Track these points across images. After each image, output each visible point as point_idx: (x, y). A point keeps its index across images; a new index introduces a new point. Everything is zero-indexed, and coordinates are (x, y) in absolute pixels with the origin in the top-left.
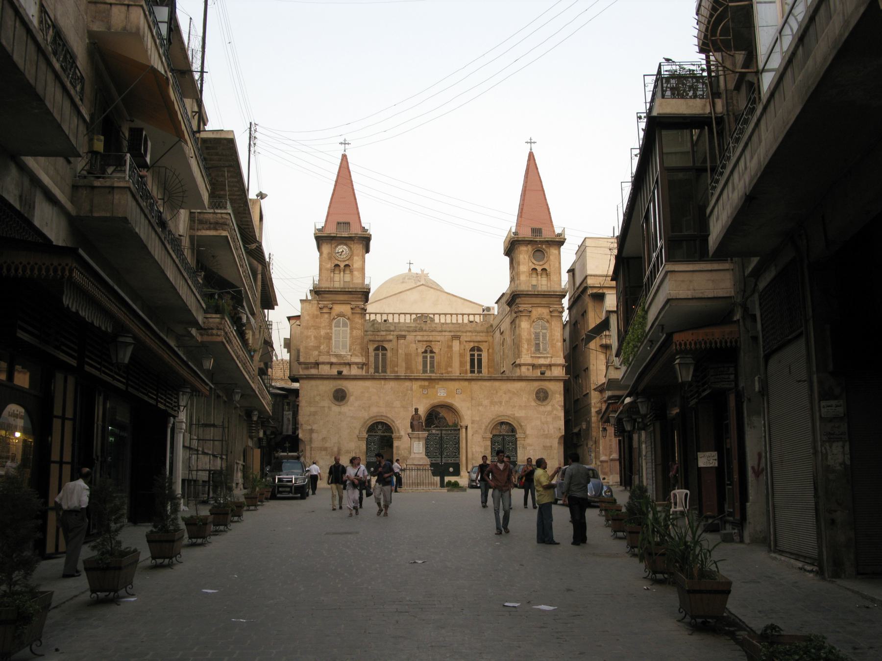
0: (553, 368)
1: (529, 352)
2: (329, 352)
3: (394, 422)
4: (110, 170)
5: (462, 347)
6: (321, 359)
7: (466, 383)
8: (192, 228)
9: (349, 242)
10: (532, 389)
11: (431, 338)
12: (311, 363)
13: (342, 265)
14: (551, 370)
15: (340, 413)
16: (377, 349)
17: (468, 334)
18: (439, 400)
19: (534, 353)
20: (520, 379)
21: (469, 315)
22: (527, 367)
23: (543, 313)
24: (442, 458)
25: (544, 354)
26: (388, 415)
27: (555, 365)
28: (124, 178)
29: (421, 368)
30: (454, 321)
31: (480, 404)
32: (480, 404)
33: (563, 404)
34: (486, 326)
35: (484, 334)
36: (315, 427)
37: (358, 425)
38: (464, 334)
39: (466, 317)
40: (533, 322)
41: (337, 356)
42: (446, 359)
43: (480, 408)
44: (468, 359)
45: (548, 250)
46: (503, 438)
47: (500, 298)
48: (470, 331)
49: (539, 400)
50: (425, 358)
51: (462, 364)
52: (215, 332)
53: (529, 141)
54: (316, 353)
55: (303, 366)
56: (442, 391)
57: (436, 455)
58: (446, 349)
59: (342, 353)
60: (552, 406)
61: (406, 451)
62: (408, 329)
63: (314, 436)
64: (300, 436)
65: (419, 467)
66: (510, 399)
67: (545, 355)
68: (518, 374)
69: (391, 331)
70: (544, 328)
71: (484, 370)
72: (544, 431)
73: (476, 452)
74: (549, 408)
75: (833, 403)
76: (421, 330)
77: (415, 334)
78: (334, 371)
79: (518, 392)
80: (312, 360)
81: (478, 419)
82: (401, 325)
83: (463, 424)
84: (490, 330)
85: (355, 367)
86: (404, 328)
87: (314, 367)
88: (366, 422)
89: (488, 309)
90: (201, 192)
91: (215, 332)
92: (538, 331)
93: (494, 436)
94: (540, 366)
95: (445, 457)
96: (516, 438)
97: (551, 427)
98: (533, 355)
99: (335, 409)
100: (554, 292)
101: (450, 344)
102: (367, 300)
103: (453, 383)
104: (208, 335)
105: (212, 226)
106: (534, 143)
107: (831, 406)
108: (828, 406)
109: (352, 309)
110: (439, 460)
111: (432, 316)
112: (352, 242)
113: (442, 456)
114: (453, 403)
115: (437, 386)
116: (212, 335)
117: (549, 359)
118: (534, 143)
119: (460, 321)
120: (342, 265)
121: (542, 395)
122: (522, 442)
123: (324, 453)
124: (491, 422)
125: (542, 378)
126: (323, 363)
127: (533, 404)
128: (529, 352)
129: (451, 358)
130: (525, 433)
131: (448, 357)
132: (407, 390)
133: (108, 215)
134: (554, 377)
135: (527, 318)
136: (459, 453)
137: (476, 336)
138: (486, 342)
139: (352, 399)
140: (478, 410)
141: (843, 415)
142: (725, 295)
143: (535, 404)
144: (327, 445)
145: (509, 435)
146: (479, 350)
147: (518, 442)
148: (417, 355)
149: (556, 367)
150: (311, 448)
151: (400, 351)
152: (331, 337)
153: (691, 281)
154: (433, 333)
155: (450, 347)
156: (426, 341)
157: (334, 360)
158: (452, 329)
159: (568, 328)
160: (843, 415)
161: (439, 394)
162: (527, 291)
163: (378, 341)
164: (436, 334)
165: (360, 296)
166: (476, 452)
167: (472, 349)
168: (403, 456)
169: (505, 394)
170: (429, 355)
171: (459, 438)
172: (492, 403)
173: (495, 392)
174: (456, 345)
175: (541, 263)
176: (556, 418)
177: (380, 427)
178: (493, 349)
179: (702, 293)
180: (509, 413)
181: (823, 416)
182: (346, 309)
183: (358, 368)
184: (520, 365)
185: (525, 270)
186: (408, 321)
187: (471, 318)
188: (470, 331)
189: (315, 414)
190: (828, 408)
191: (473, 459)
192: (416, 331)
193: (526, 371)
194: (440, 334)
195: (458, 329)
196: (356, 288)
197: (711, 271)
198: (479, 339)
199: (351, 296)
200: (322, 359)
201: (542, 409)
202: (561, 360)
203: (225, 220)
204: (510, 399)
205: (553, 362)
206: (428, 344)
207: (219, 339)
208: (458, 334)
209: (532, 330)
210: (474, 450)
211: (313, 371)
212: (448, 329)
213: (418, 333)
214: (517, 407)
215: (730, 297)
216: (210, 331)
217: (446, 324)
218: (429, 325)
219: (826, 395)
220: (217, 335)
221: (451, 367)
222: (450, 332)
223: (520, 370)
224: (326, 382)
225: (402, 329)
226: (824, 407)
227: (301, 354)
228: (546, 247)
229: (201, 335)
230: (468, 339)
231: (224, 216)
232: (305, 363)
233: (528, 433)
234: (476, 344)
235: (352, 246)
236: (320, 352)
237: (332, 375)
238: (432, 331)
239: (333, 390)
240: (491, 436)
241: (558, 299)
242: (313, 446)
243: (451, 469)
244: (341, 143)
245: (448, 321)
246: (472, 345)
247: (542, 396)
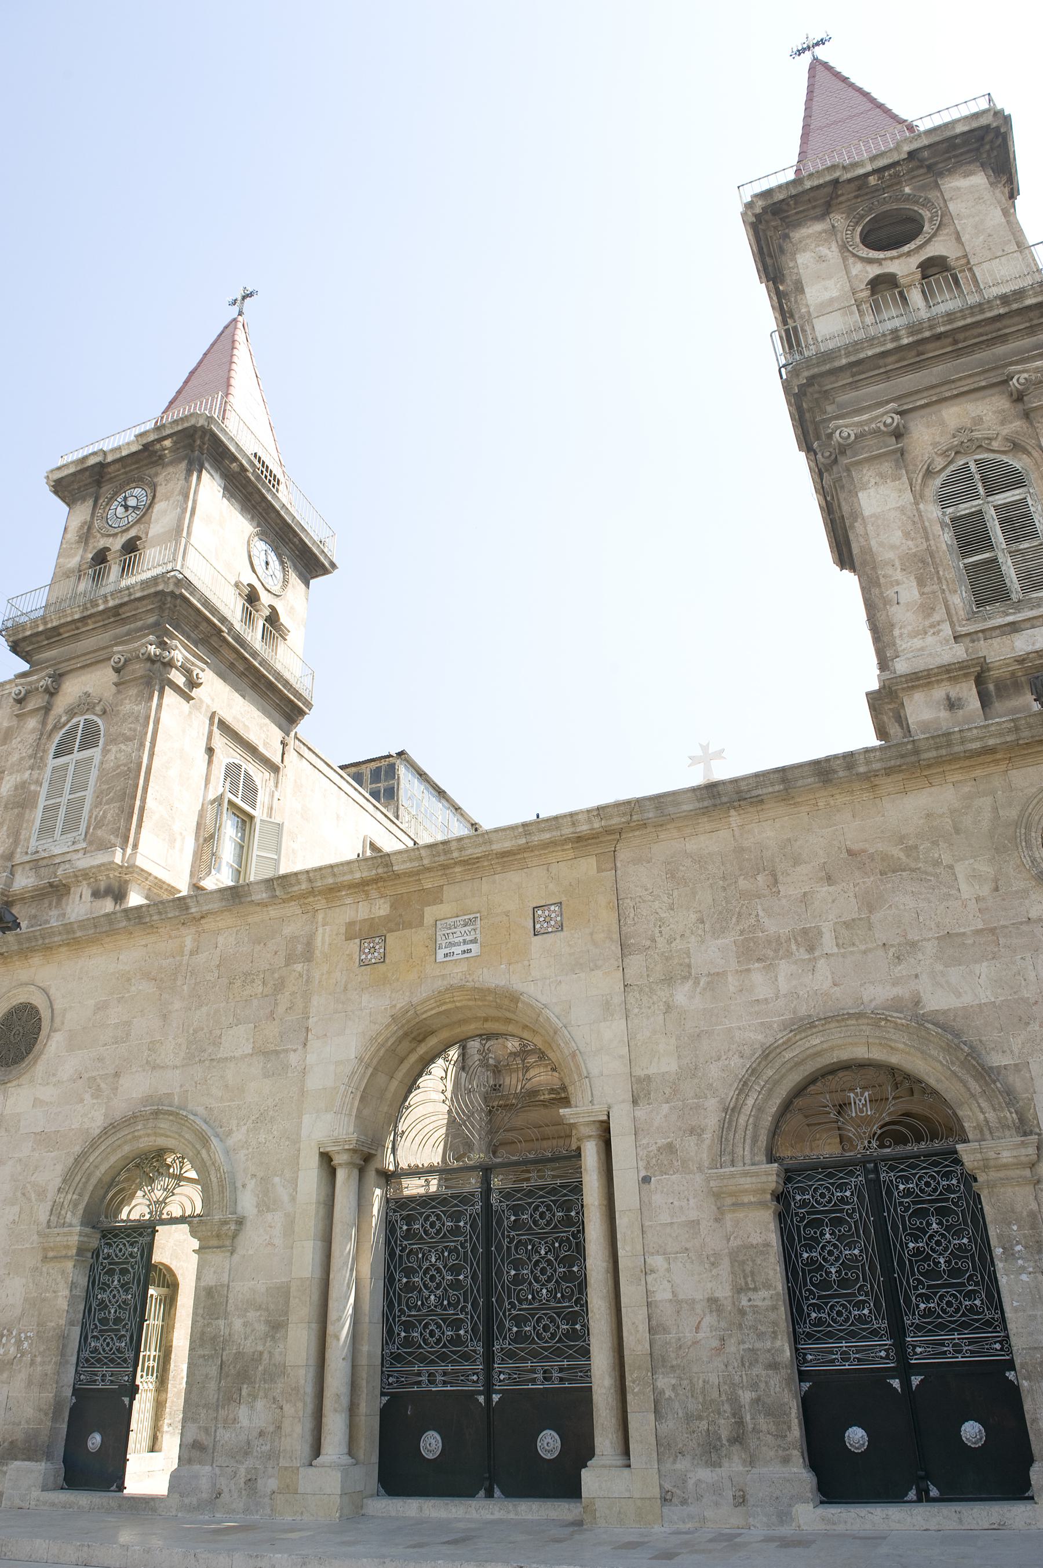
1: (936, 617)
13: (116, 544)
19: (971, 617)
22: (939, 693)
23: (979, 420)
24: (489, 1359)
40: (929, 473)
43: (682, 995)
45: (933, 195)
46: (875, 1185)
57: (456, 1341)
59: (57, 851)
61: (252, 1315)
66: (870, 903)
73: (677, 1302)
79: (910, 850)
92: (965, 508)
93: (789, 1175)
95: (511, 1355)
98: (962, 630)
100: (1004, 299)
109: (117, 670)
112: (159, 469)
113: (488, 1345)
124: (754, 1071)
128: (940, 614)
132: (289, 960)
135: (887, 467)
140: (668, 1008)
152: (36, 794)
161: (440, 954)
166: (677, 1302)
168: (239, 1355)
169: (829, 879)
185: (835, 294)
191: (656, 1361)
193: (944, 714)
204: (870, 903)
209: (932, 511)
210: (662, 1294)
214: (930, 948)
228: (923, 188)
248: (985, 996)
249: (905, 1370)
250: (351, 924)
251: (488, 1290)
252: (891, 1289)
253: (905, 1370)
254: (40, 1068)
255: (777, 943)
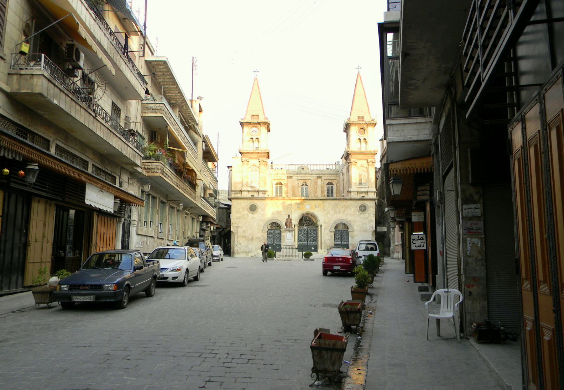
0: (369, 193)
2: (247, 185)
3: (282, 222)
4: (32, 64)
5: (323, 183)
6: (243, 189)
7: (321, 202)
8: (142, 112)
9: (258, 126)
10: (357, 205)
11: (306, 178)
12: (238, 191)
14: (368, 194)
15: (253, 217)
16: (277, 184)
17: (326, 175)
18: (306, 211)
20: (351, 200)
21: (326, 165)
22: (354, 193)
25: (364, 186)
26: (279, 219)
27: (370, 192)
28: (40, 69)
29: (301, 194)
30: (318, 169)
31: (329, 213)
32: (329, 213)
33: (374, 213)
34: (336, 171)
35: (334, 176)
36: (240, 225)
37: (262, 224)
38: (324, 176)
39: (325, 167)
41: (251, 187)
42: (314, 189)
43: (329, 215)
44: (326, 189)
47: (342, 157)
48: (327, 174)
49: (361, 211)
50: (302, 189)
51: (322, 192)
52: (155, 170)
53: (358, 67)
54: (241, 185)
55: (234, 192)
56: (308, 206)
58: (314, 184)
60: (368, 214)
62: (293, 173)
63: (239, 229)
64: (232, 230)
65: (289, 247)
67: (365, 187)
68: (349, 197)
69: (284, 174)
70: (363, 171)
71: (335, 195)
72: (364, 228)
74: (367, 215)
75: (473, 206)
76: (301, 173)
77: (297, 175)
78: (250, 195)
80: (239, 189)
81: (327, 221)
82: (290, 171)
83: (319, 224)
84: (337, 173)
85: (261, 193)
86: (292, 173)
87: (239, 193)
88: (266, 223)
89: (338, 162)
90: (137, 90)
91: (155, 170)
92: (361, 173)
94: (362, 192)
96: (348, 232)
97: (368, 226)
98: (358, 186)
99: (250, 215)
101: (316, 181)
102: (268, 157)
103: (314, 201)
104: (152, 172)
105: (154, 111)
106: (361, 68)
107: (471, 209)
108: (470, 209)
110: (306, 243)
111: (306, 166)
114: (314, 212)
115: (305, 203)
116: (154, 172)
117: (367, 188)
118: (361, 68)
119: (322, 169)
120: (254, 138)
121: (363, 208)
122: (352, 234)
123: (244, 239)
125: (363, 199)
126: (244, 191)
127: (358, 213)
129: (316, 189)
130: (353, 229)
131: (315, 188)
133: (30, 91)
134: (370, 198)
135: (354, 166)
136: (317, 240)
137: (330, 176)
138: (335, 180)
139: (259, 210)
140: (327, 216)
141: (480, 215)
142: (425, 139)
143: (359, 213)
144: (246, 235)
145: (344, 230)
146: (332, 184)
147: (349, 234)
148: (298, 187)
149: (371, 193)
150: (237, 236)
151: (289, 185)
153: (403, 130)
154: (307, 175)
155: (316, 183)
156: (303, 179)
157: (250, 189)
158: (317, 173)
159: (380, 173)
160: (480, 215)
162: (355, 151)
163: (277, 179)
164: (309, 175)
165: (264, 155)
167: (328, 184)
170: (304, 187)
171: (317, 231)
172: (335, 212)
173: (337, 206)
174: (319, 180)
175: (363, 135)
176: (370, 221)
177: (274, 225)
178: (339, 183)
179: (410, 138)
180: (344, 218)
181: (464, 215)
182: (256, 162)
183: (263, 193)
184: (350, 192)
186: (294, 169)
187: (328, 167)
188: (327, 174)
189: (239, 218)
190: (469, 210)
191: (324, 243)
192: (298, 174)
194: (311, 175)
195: (320, 173)
196: (262, 151)
197: (417, 123)
198: (332, 178)
199: (259, 155)
200: (245, 188)
201: (363, 216)
202: (374, 190)
203: (161, 108)
205: (369, 190)
206: (304, 181)
207: (158, 175)
208: (321, 175)
211: (239, 195)
212: (315, 173)
213: (299, 175)
215: (428, 140)
216: (153, 170)
217: (314, 170)
218: (305, 171)
219: (466, 201)
220: (157, 172)
221: (316, 193)
222: (316, 174)
223: (351, 194)
224: (246, 201)
225: (290, 173)
226: (465, 209)
227: (232, 186)
229: (148, 172)
230: (326, 178)
231: (161, 105)
232: (234, 191)
233: (355, 229)
234: (330, 181)
235: (259, 128)
236: (242, 185)
237: (248, 197)
238: (307, 174)
239: (250, 205)
240: (267, 230)
241: (372, 155)
242: (238, 235)
243: (313, 248)
244: (254, 72)
245: (315, 169)
246: (328, 181)
247: (363, 209)
248: (352, 219)
249: (341, 244)
250: (296, 203)
251: (307, 237)
252: (341, 239)
253: (341, 244)
254: (258, 212)
255: (337, 212)
